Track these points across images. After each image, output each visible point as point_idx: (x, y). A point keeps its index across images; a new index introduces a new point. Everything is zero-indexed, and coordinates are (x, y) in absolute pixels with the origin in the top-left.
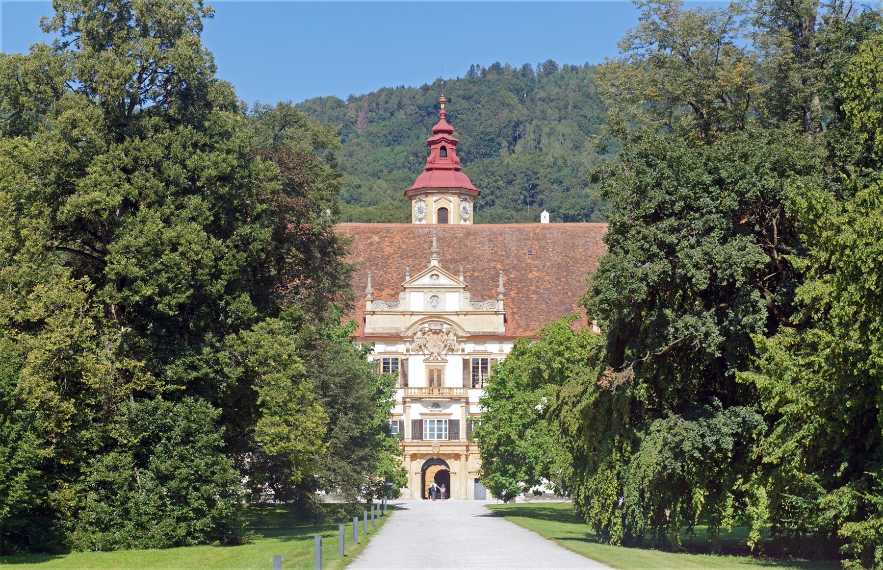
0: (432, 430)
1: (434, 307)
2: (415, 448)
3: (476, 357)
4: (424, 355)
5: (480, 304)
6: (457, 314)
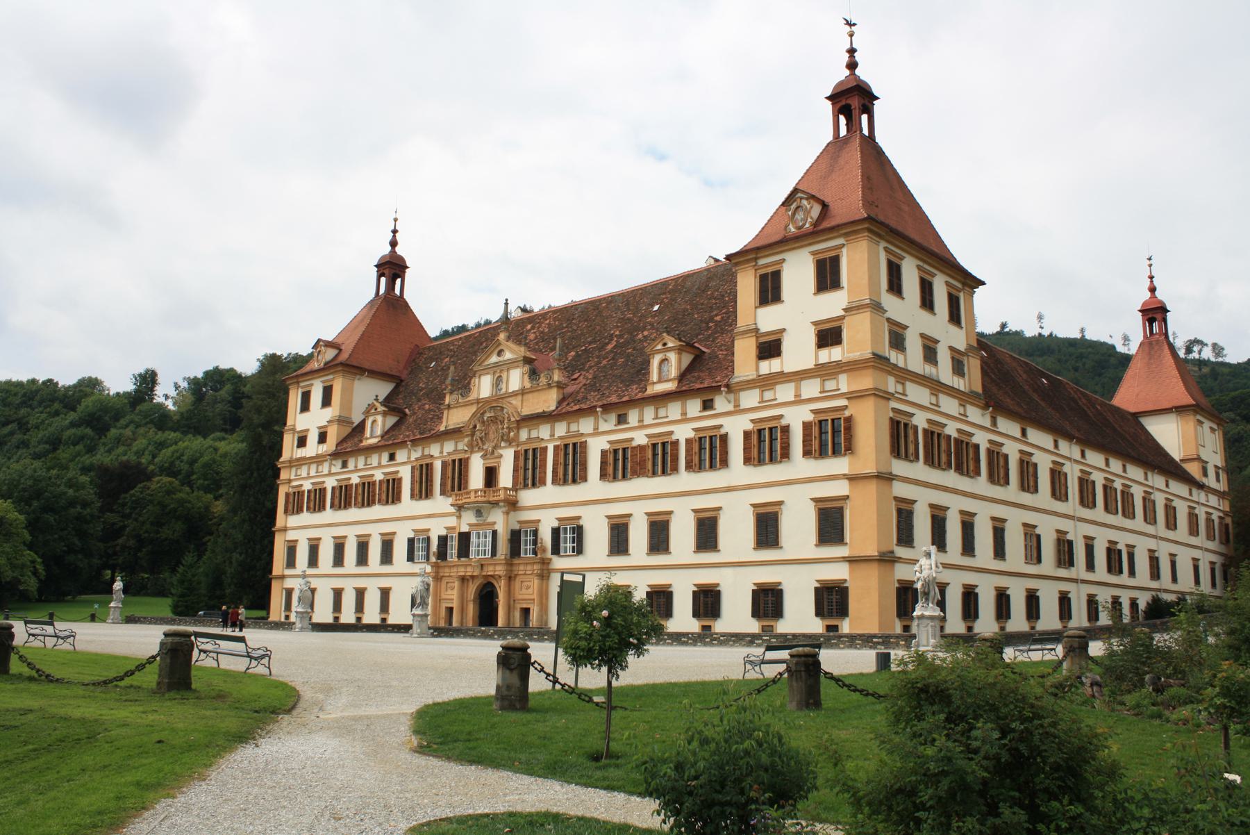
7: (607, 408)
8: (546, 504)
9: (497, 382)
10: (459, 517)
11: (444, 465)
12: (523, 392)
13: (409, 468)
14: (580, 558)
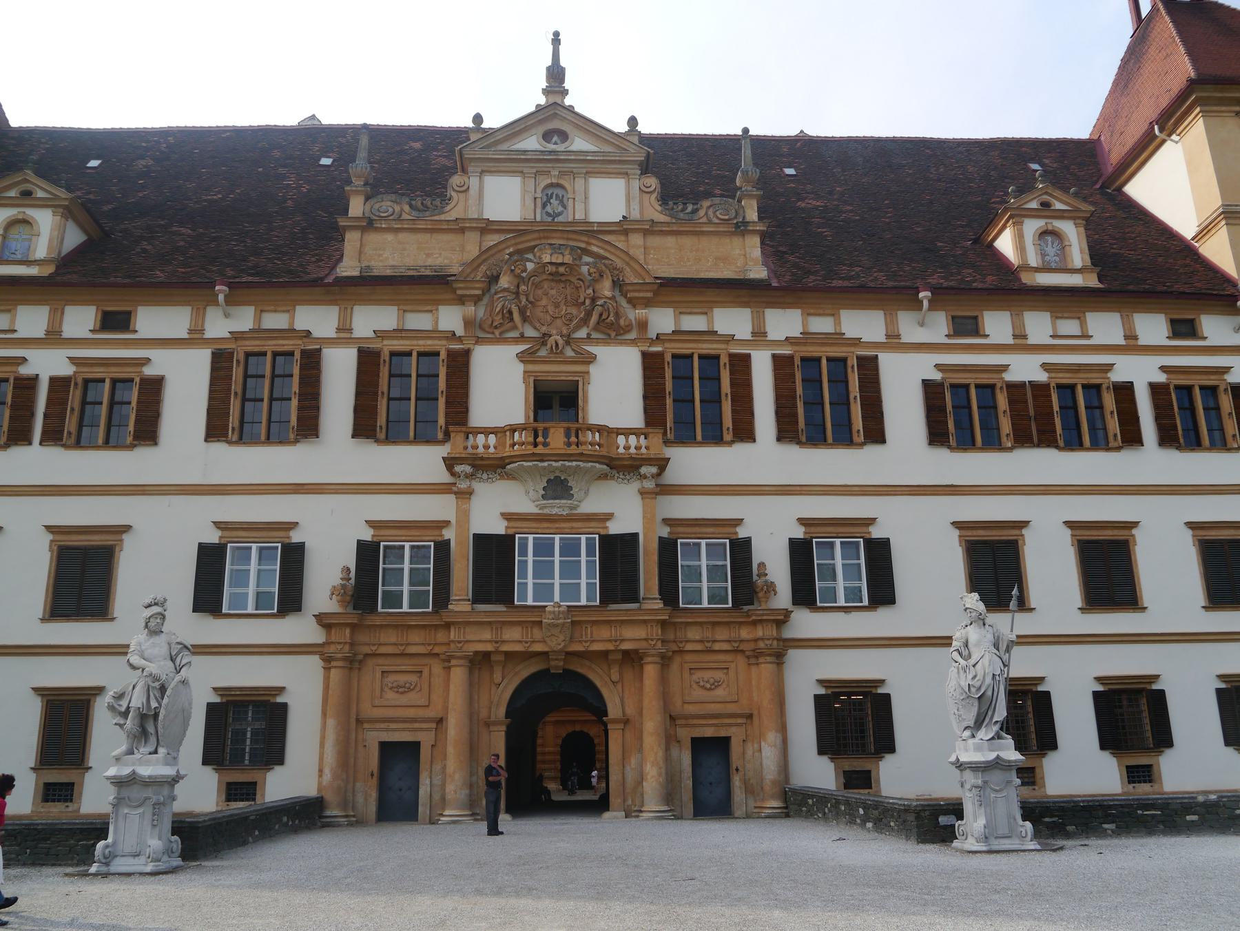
0: (543, 570)
3: (684, 348)
4: (522, 338)
6: (624, 227)
7: (941, 297)
8: (761, 486)
9: (553, 194)
10: (466, 495)
11: (368, 361)
12: (650, 229)
13: (201, 359)
14: (883, 613)
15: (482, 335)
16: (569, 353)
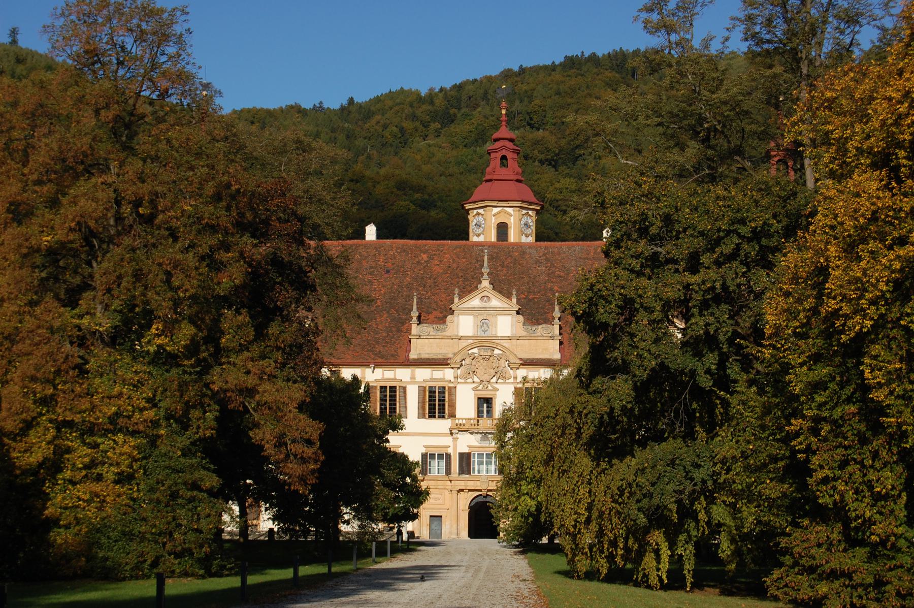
0: (480, 463)
1: (485, 331)
2: (462, 483)
5: (534, 328)
11: (422, 389)
15: (459, 380)
16: (490, 388)
